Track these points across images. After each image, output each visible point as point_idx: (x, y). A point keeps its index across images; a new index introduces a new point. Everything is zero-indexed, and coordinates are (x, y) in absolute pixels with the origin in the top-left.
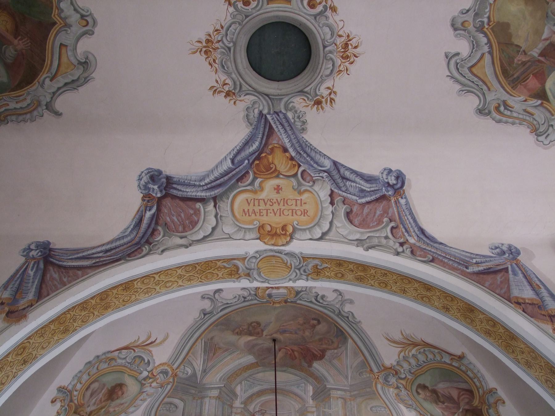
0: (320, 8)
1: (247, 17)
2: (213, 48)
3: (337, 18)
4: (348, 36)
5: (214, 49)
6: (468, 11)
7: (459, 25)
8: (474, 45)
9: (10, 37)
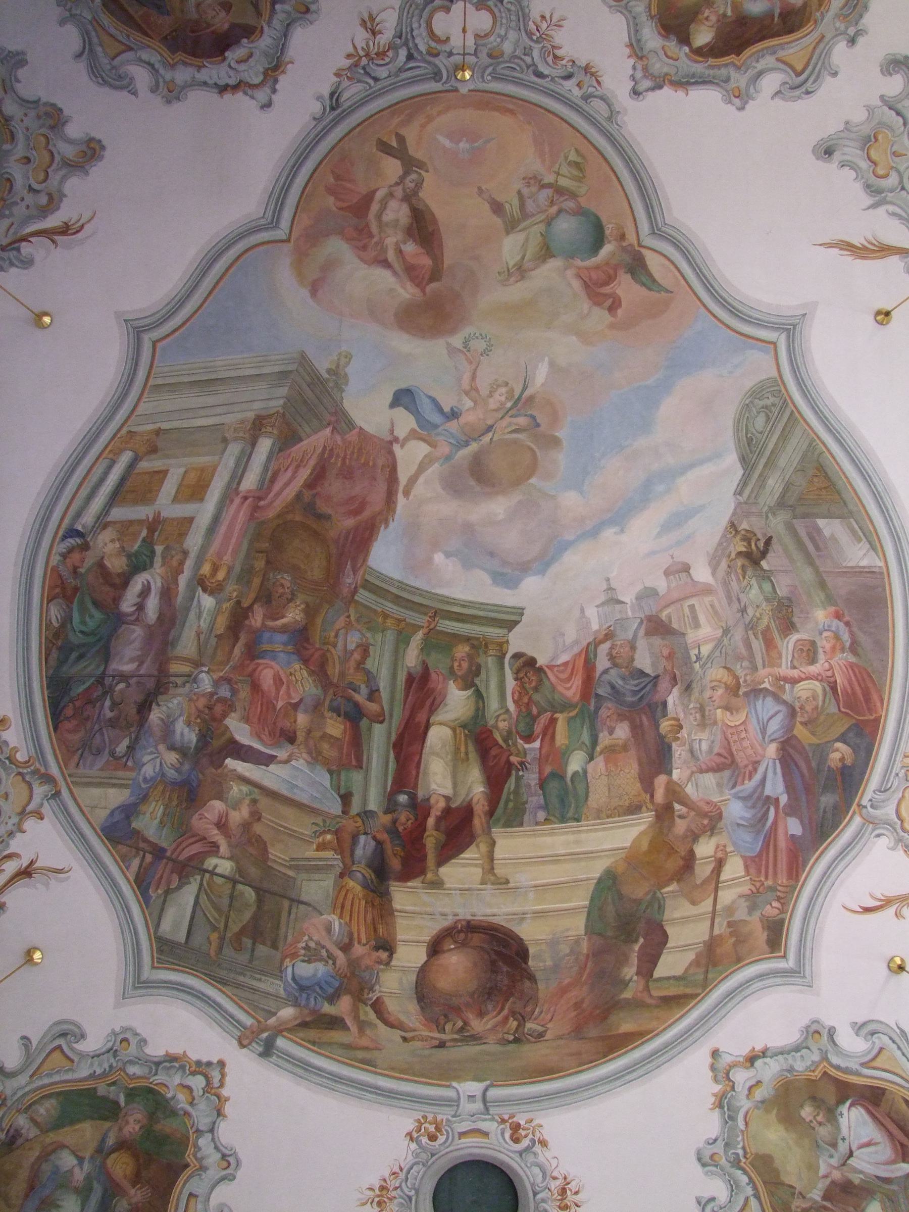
0: (526, 1143)
1: (433, 1155)
2: (388, 1198)
3: (548, 1155)
4: (565, 1178)
5: (390, 1199)
6: (715, 1140)
7: (707, 1159)
8: (732, 1186)
9: (126, 1184)
